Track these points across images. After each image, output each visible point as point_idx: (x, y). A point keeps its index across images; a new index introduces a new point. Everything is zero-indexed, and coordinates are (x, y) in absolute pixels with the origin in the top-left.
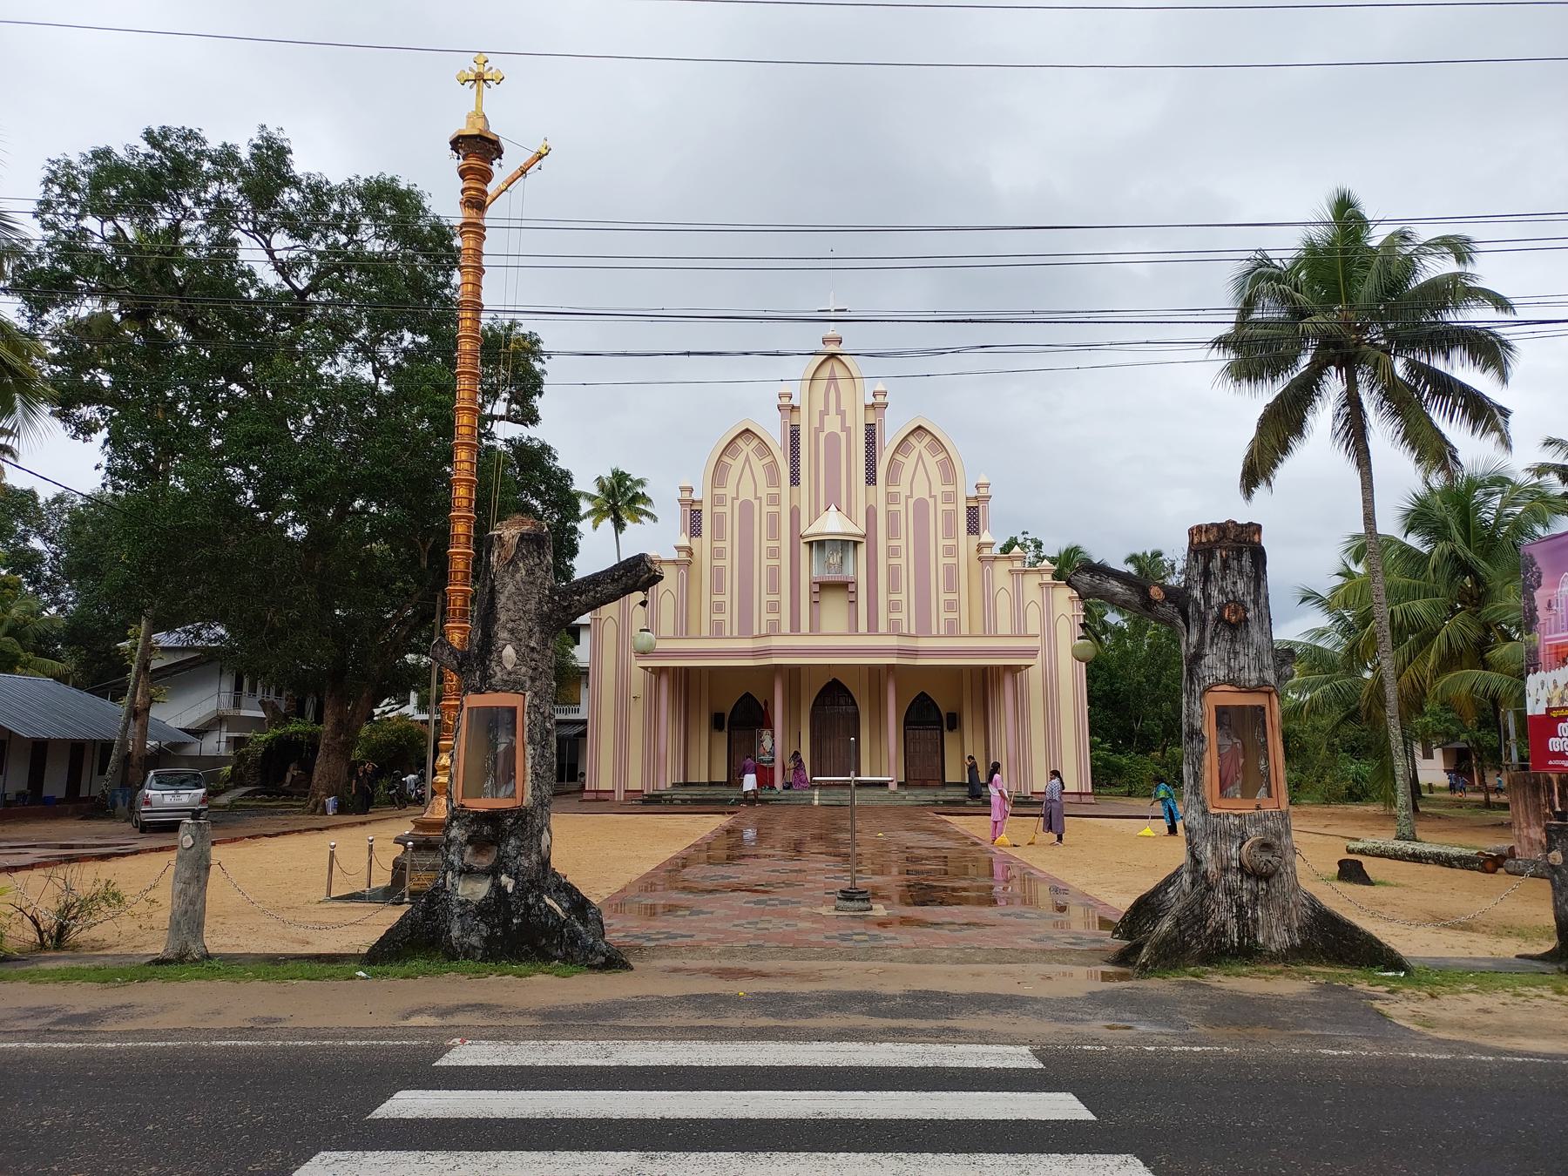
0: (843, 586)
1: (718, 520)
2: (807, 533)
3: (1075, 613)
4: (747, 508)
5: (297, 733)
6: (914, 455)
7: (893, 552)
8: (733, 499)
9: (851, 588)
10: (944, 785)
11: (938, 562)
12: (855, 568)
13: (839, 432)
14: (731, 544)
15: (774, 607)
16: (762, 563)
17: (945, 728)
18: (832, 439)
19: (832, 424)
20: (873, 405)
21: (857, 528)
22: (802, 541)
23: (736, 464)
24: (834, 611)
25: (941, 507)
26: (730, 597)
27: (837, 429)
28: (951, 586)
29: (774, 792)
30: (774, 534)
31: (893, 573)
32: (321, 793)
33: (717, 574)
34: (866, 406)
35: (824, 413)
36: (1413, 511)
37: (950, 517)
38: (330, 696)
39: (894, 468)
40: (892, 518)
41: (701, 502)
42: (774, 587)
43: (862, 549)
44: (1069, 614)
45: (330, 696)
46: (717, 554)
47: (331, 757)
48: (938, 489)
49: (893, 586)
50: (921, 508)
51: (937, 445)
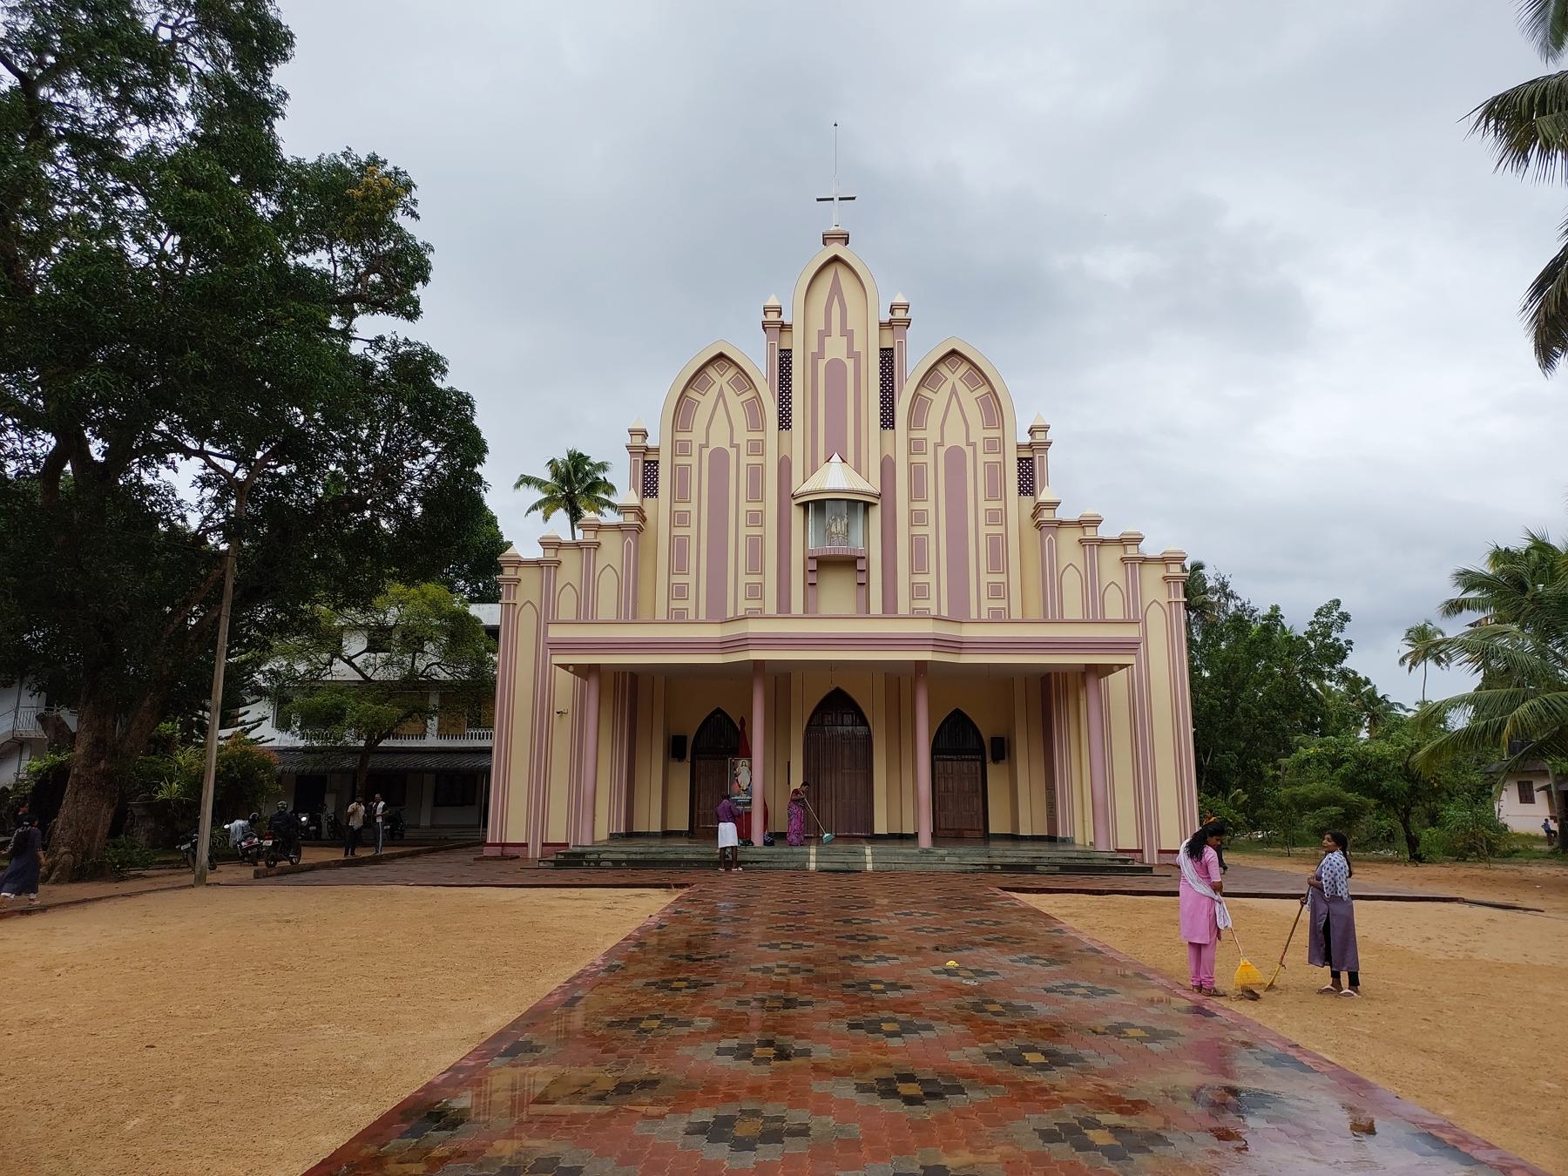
0: (850, 563)
1: (681, 475)
2: (800, 490)
3: (1173, 599)
4: (720, 458)
6: (946, 389)
7: (917, 518)
9: (861, 565)
10: (987, 837)
11: (979, 531)
12: (867, 539)
14: (697, 506)
15: (756, 592)
16: (739, 533)
17: (988, 759)
18: (836, 367)
19: (836, 348)
21: (874, 487)
22: (794, 502)
23: (705, 402)
25: (983, 458)
26: (695, 578)
27: (841, 354)
28: (997, 560)
29: (750, 849)
30: (756, 493)
31: (918, 545)
32: (63, 849)
33: (679, 548)
34: (881, 324)
35: (825, 334)
37: (994, 474)
40: (916, 473)
42: (756, 565)
43: (875, 515)
44: (1164, 602)
46: (679, 519)
47: (82, 795)
48: (979, 434)
50: (955, 459)
51: (977, 375)
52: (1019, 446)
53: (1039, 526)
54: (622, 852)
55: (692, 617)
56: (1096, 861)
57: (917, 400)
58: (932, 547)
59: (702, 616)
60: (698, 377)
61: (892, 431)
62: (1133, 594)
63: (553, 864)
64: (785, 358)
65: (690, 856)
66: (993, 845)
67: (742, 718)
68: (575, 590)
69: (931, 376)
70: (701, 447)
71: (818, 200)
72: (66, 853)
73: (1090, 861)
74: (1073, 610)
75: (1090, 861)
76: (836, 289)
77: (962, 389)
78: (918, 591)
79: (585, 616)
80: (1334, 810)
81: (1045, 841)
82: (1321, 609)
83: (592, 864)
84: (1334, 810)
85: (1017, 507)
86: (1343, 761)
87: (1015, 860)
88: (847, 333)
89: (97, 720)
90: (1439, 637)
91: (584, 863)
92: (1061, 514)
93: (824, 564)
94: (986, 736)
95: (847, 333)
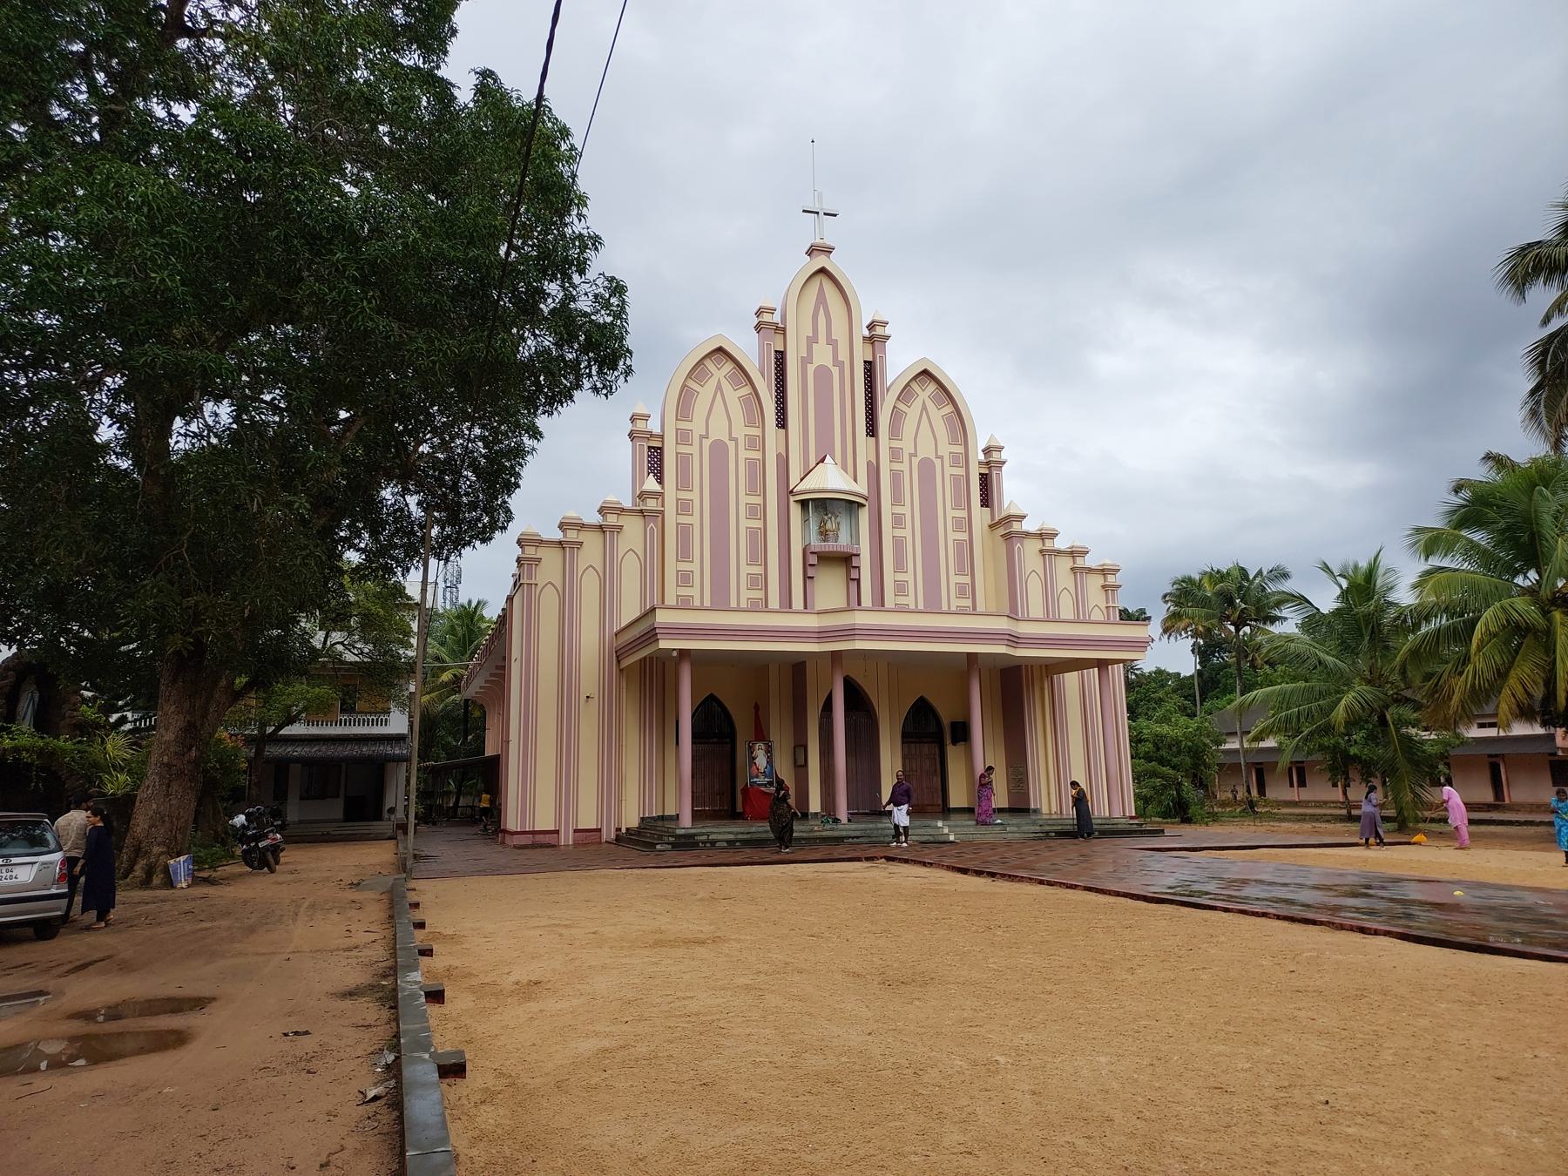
0: (846, 560)
1: (683, 461)
3: (1110, 604)
4: (719, 450)
5: (16, 750)
6: (917, 405)
7: (898, 521)
8: (702, 437)
10: (946, 811)
11: (949, 537)
12: (854, 536)
13: (830, 366)
15: (761, 582)
16: (741, 525)
17: (948, 740)
18: (822, 372)
19: (822, 355)
21: (862, 488)
22: (792, 499)
23: (705, 393)
24: (830, 588)
25: (949, 471)
26: (700, 564)
27: (829, 363)
29: (840, 826)
31: (899, 544)
32: (156, 850)
33: (684, 532)
34: (864, 338)
35: (813, 340)
36: (1464, 506)
37: (961, 484)
38: (174, 681)
39: (897, 416)
40: (896, 477)
43: (864, 516)
44: (1103, 606)
45: (174, 681)
46: (684, 507)
47: (175, 787)
48: (946, 449)
49: (899, 566)
50: (927, 468)
51: (945, 393)
53: (1008, 537)
54: (729, 833)
55: (697, 603)
56: (1119, 826)
57: (897, 416)
58: (910, 549)
59: (707, 603)
60: (698, 371)
61: (873, 439)
62: (1079, 601)
63: (670, 846)
64: (781, 358)
66: (953, 816)
67: (756, 704)
68: (598, 573)
69: (906, 394)
70: (911, 455)
71: (804, 211)
72: (162, 853)
73: (1115, 826)
74: (1036, 610)
75: (1115, 826)
76: (821, 300)
77: (930, 406)
78: (901, 588)
79: (720, 602)
81: (1006, 812)
83: (708, 845)
85: (980, 516)
87: (1060, 828)
88: (832, 342)
89: (188, 701)
91: (701, 845)
92: (1028, 526)
93: (827, 559)
94: (946, 721)
95: (832, 342)
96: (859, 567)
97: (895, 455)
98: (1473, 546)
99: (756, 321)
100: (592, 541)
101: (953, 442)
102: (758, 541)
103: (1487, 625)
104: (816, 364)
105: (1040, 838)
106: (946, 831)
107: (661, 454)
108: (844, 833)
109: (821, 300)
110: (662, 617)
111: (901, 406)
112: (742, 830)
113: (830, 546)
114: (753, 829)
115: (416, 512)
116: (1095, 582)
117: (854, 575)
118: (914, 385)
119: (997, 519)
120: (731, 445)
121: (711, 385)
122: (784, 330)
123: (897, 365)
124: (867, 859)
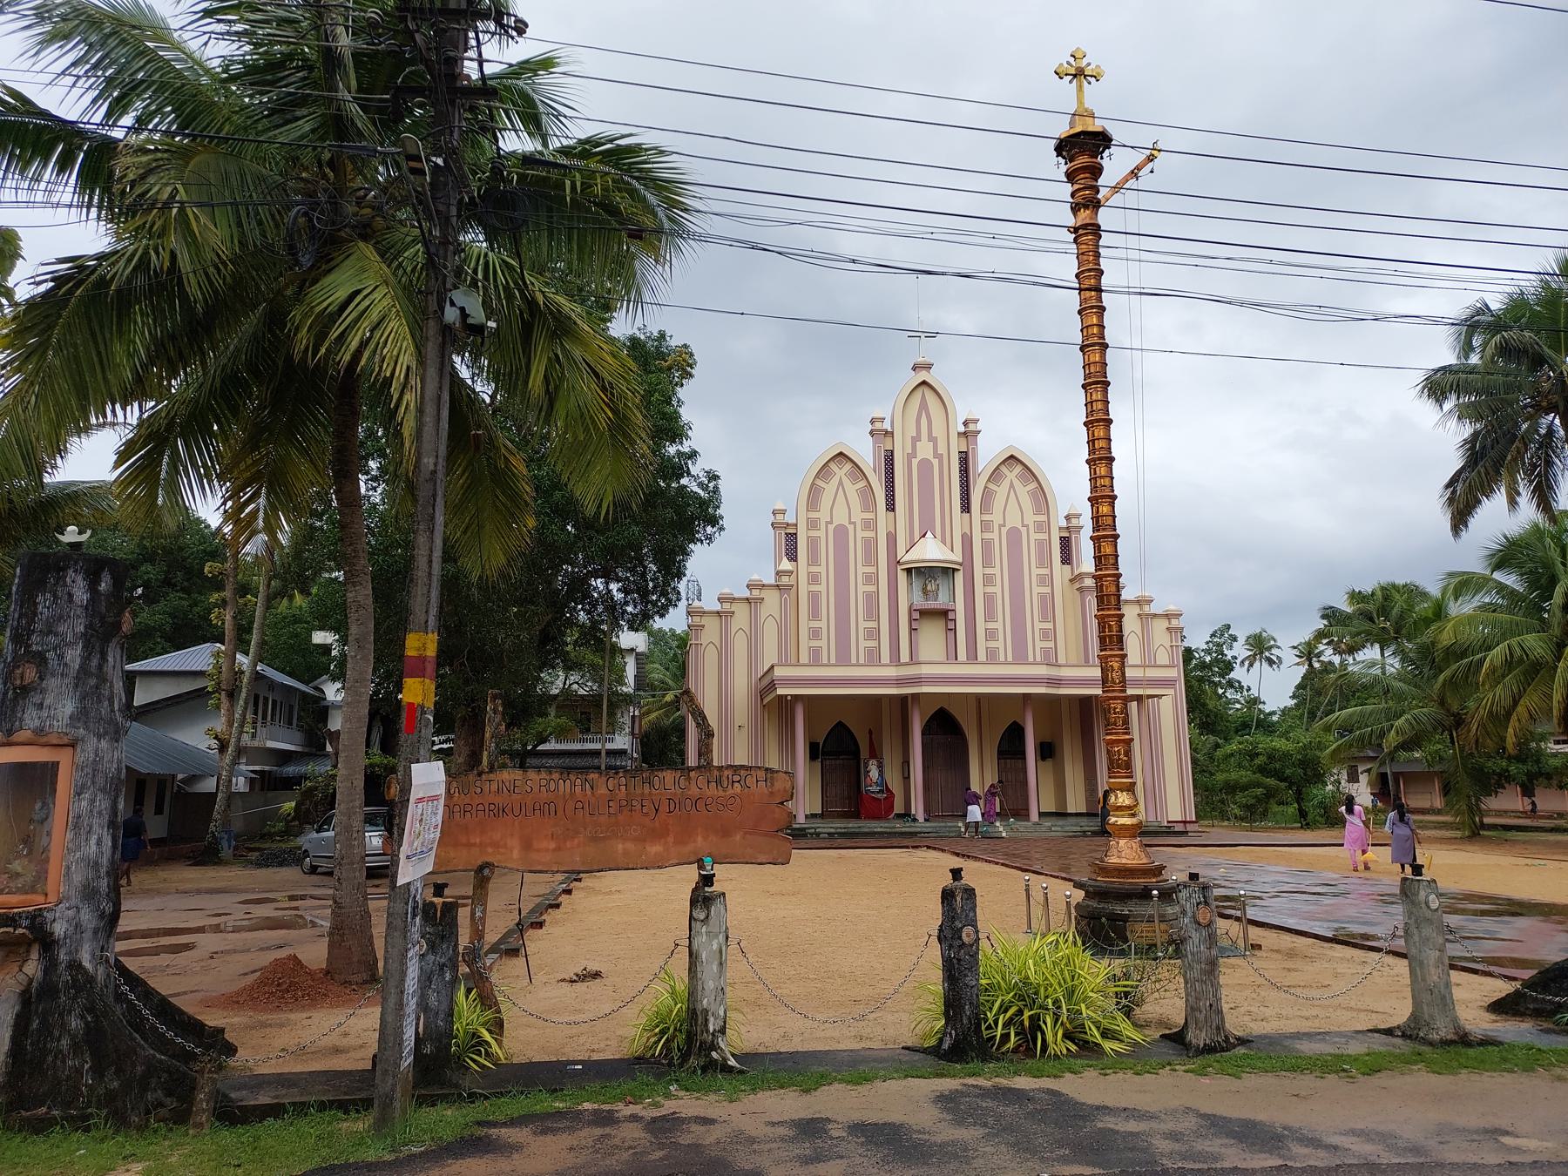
0: (944, 614)
1: (813, 544)
3: (1174, 644)
4: (841, 532)
7: (988, 580)
8: (827, 523)
9: (951, 616)
11: (1033, 591)
14: (826, 568)
15: (874, 634)
16: (859, 590)
18: (925, 465)
19: (925, 450)
20: (965, 433)
21: (957, 556)
22: (899, 568)
23: (830, 488)
24: (932, 639)
25: (1034, 536)
26: (827, 622)
28: (1047, 609)
29: (917, 824)
31: (989, 599)
33: (814, 598)
34: (959, 434)
36: (1501, 551)
37: (1043, 549)
39: (987, 495)
40: (987, 546)
41: (796, 525)
43: (959, 577)
44: (1168, 645)
46: (814, 579)
48: (1031, 519)
49: (990, 615)
50: (1014, 536)
51: (1029, 473)
52: (1060, 528)
58: (1000, 602)
60: (824, 472)
64: (890, 459)
65: (879, 830)
69: (996, 475)
76: (924, 406)
80: (1260, 791)
82: (1215, 632)
84: (1260, 791)
86: (1257, 754)
90: (1272, 643)
93: (926, 614)
96: (955, 620)
97: (986, 526)
98: (1501, 588)
99: (870, 427)
100: (741, 611)
101: (1038, 512)
102: (872, 601)
103: (1491, 660)
104: (918, 459)
105: (1075, 836)
106: (1001, 829)
107: (796, 538)
108: (919, 830)
109: (924, 406)
110: (779, 672)
111: (991, 486)
112: (842, 826)
113: (931, 604)
114: (850, 825)
115: (619, 596)
116: (1160, 626)
117: (951, 626)
118: (1003, 468)
119: (1076, 573)
120: (851, 528)
121: (835, 482)
122: (892, 433)
123: (986, 454)
124: (913, 847)
